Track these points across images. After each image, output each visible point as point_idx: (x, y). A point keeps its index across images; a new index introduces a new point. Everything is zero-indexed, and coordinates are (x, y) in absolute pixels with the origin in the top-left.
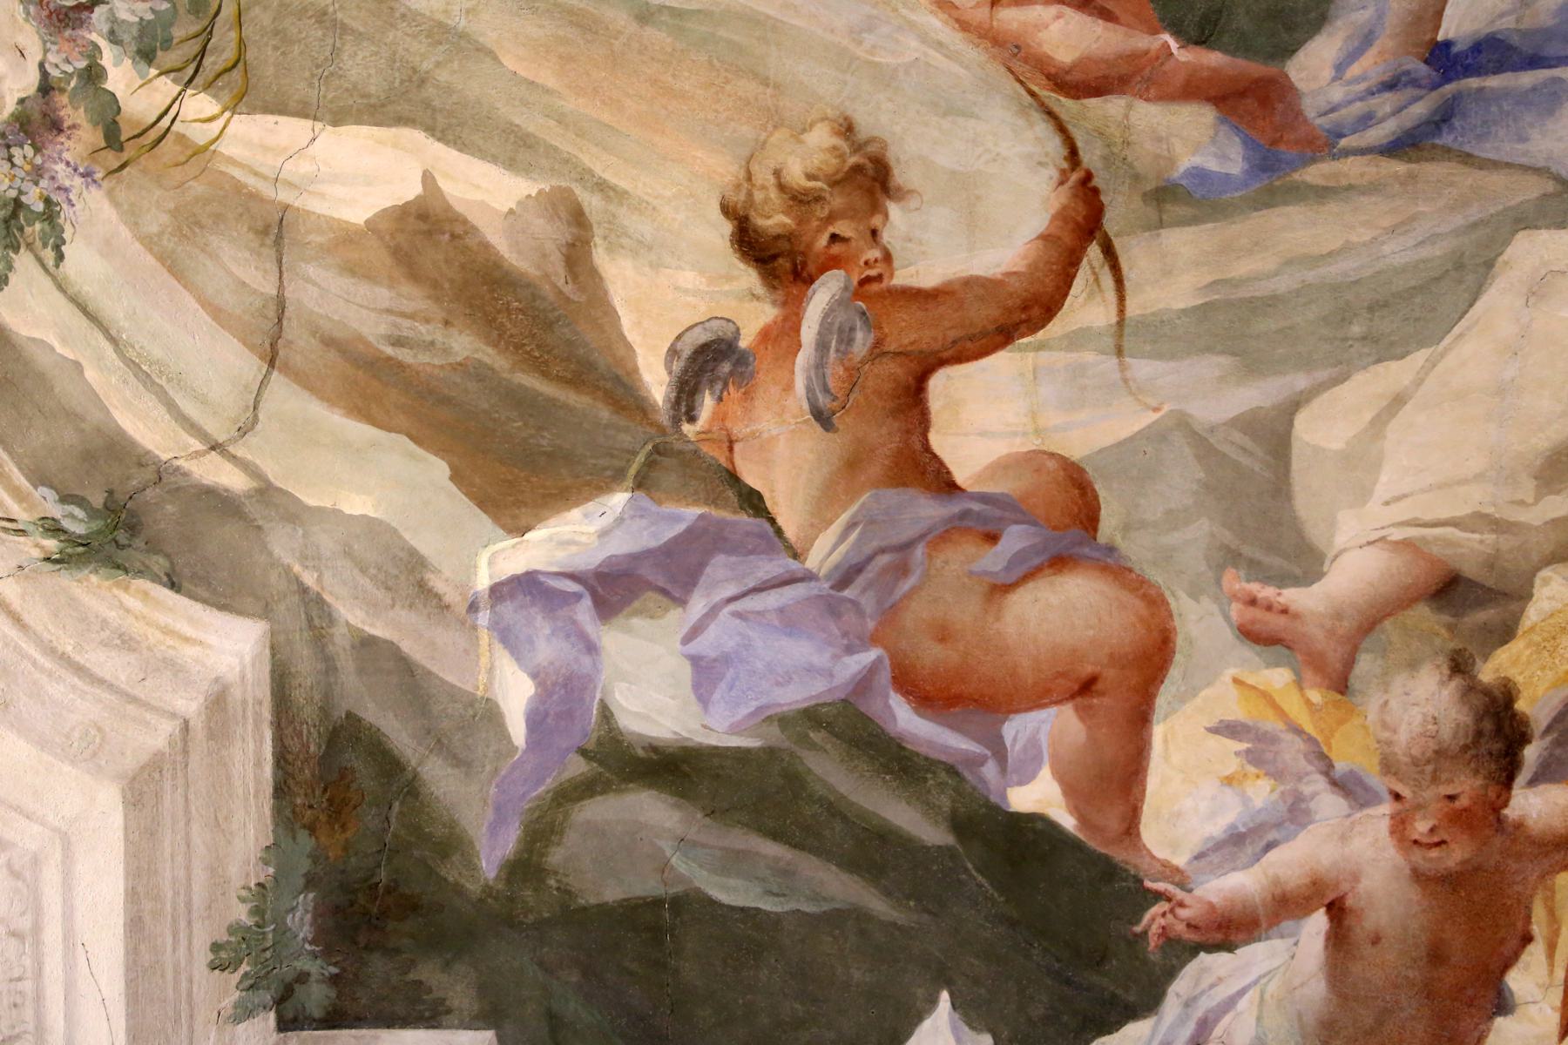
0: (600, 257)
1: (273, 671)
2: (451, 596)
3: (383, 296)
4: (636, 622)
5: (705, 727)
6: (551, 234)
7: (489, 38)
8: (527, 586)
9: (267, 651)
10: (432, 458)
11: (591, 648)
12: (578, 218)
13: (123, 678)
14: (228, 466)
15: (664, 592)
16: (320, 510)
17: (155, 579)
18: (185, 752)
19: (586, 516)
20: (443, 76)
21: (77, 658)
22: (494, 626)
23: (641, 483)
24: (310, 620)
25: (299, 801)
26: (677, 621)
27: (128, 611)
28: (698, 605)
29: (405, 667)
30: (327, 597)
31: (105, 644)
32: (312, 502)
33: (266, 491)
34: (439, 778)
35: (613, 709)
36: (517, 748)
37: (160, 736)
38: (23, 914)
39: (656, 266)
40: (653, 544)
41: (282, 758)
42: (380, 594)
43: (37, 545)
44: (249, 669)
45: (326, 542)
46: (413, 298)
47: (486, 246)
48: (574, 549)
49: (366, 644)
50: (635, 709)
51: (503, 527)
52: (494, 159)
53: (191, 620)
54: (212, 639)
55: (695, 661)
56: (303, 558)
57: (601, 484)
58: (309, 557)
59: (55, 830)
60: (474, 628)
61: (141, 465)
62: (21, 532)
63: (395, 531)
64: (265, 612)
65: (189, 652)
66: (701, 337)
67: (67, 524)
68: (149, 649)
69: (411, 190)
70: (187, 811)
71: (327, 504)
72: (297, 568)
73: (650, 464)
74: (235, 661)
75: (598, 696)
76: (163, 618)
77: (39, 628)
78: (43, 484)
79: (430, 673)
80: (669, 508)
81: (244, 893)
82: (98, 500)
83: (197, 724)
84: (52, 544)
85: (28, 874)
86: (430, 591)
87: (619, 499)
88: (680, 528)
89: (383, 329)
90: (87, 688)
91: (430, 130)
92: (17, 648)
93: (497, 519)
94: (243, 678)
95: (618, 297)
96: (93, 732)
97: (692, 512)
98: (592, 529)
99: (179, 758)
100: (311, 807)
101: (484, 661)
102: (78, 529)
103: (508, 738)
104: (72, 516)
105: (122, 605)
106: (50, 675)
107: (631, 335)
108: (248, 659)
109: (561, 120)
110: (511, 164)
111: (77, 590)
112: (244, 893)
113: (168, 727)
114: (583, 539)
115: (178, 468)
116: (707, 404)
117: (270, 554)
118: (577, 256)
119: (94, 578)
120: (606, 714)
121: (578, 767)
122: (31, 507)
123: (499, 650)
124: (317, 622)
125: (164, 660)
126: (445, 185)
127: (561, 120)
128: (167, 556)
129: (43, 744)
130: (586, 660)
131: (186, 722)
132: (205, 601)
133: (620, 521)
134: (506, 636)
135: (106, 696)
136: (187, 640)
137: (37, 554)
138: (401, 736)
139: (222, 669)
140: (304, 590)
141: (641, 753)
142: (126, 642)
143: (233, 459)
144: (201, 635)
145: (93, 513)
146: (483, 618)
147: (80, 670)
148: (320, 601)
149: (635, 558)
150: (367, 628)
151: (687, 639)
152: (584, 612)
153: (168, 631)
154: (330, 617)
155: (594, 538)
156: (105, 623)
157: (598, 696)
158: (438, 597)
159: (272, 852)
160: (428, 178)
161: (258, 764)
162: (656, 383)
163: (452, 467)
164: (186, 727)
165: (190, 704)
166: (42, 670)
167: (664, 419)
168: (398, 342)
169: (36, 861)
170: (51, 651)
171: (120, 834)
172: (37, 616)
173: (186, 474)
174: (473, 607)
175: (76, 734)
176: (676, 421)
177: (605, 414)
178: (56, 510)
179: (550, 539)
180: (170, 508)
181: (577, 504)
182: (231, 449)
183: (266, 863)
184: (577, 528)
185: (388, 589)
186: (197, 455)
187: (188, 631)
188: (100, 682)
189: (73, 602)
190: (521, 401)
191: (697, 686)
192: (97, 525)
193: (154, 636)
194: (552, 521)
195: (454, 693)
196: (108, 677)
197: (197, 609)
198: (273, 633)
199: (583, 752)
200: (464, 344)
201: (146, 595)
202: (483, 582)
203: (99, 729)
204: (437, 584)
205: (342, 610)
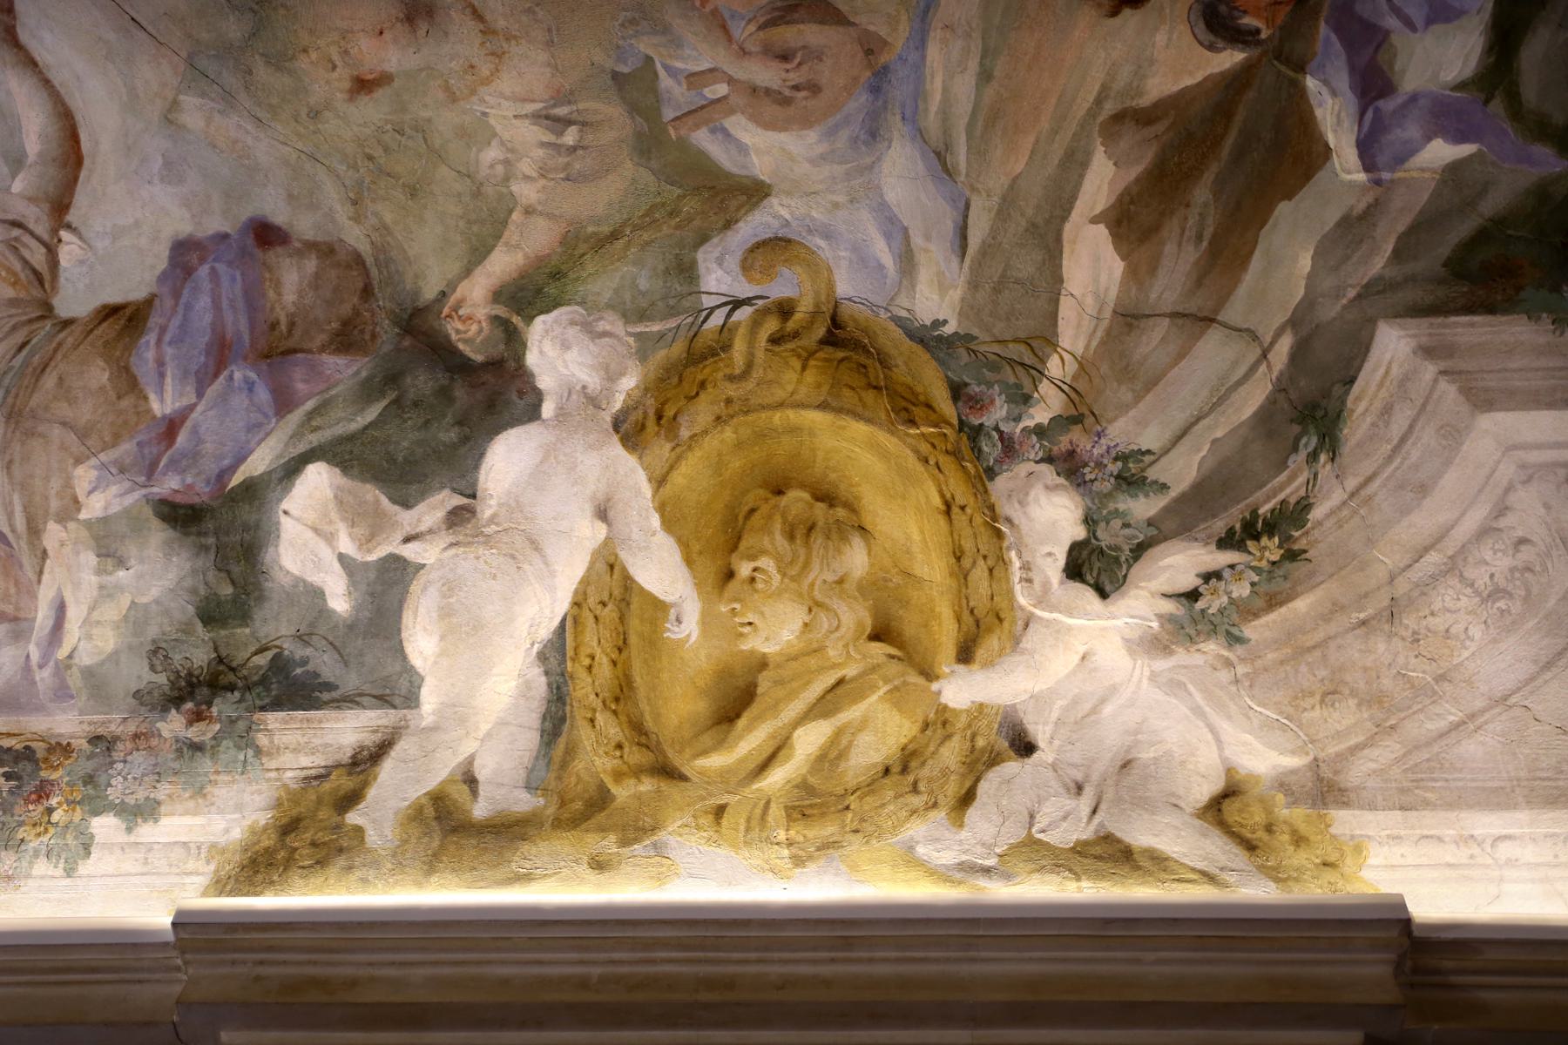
0: (1145, 101)
1: (1412, 317)
2: (1369, 198)
3: (1170, 248)
4: (1397, 67)
5: (1478, 12)
6: (1130, 137)
7: (1005, 181)
8: (1367, 148)
9: (1398, 320)
10: (1276, 213)
11: (1414, 98)
12: (1119, 118)
13: (1409, 413)
14: (1277, 347)
15: (1379, 46)
16: (1307, 287)
17: (1347, 392)
18: (1460, 373)
19: (1320, 105)
20: (1030, 212)
21: (1395, 442)
22: (1393, 170)
23: (1301, 68)
24: (1379, 293)
25: (1499, 298)
26: (1400, 38)
27: (1367, 410)
28: (1391, 22)
29: (1413, 229)
30: (1365, 281)
31: (1387, 424)
32: (1302, 292)
33: (1294, 322)
34: (1494, 203)
35: (1459, 80)
36: (1480, 150)
37: (1449, 391)
38: (1556, 474)
39: (1152, 62)
40: (1344, 57)
41: (1469, 310)
42: (1364, 247)
43: (1324, 466)
44: (1412, 332)
45: (1328, 283)
46: (1171, 227)
47: (1137, 180)
48: (1343, 114)
49: (1398, 255)
50: (1460, 65)
51: (1325, 163)
52: (1082, 176)
53: (1374, 370)
54: (1388, 356)
55: (1430, 22)
56: (1338, 297)
57: (1300, 93)
58: (1338, 293)
59: (1503, 455)
60: (1392, 181)
61: (1275, 402)
62: (1316, 475)
63: (1325, 236)
64: (1371, 323)
65: (1395, 371)
66: (1201, 27)
67: (1310, 449)
68: (1391, 396)
69: (1102, 231)
70: (1499, 371)
71: (1303, 283)
72: (1344, 301)
73: (1287, 62)
74: (1403, 341)
75: (1448, 92)
76: (1373, 388)
77: (1376, 465)
78: (1286, 462)
79: (1420, 212)
80: (1319, 47)
81: (1558, 333)
82: (1296, 429)
83: (1443, 365)
84: (1323, 457)
85: (1531, 471)
86: (1364, 212)
87: (1311, 83)
88: (1334, 37)
89: (1191, 248)
90: (1414, 436)
91: (1064, 219)
92: (1388, 479)
93: (1320, 167)
94: (1415, 336)
95: (1172, 87)
96: (1443, 432)
97: (1322, 24)
98: (1330, 101)
99: (1464, 377)
100: (1504, 290)
101: (1415, 174)
102: (1314, 440)
103: (1471, 156)
104: (1306, 445)
105: (1363, 414)
106: (1404, 459)
107: (1199, 77)
108: (1402, 333)
109: (1055, 132)
110: (1085, 165)
111: (1352, 442)
112: (1558, 333)
113: (1443, 385)
114: (1337, 108)
115: (1278, 379)
116: (1248, 21)
117: (1335, 319)
118: (1144, 117)
119: (1345, 431)
120: (1461, 86)
121: (1497, 106)
122: (1300, 470)
123: (1407, 165)
124: (1381, 288)
125: (1399, 387)
126: (1099, 208)
127: (1055, 132)
128: (1333, 385)
129: (1448, 463)
130: (1422, 102)
131: (1441, 372)
132: (1363, 361)
133: (1326, 82)
134: (1400, 160)
135: (1420, 424)
136: (1387, 372)
137: (1328, 467)
138: (1462, 230)
139: (1408, 350)
140: (1359, 296)
141: (1492, 60)
142: (1387, 410)
143: (1272, 344)
144: (1385, 363)
145: (1304, 432)
146: (1386, 176)
147: (1403, 440)
148: (1367, 286)
149: (1352, 69)
150: (1387, 255)
151: (1410, 25)
152: (1388, 105)
153: (1381, 385)
154: (1378, 279)
155: (1337, 100)
156: (1374, 424)
157: (1448, 92)
158: (1369, 207)
159: (1533, 315)
160: (1095, 220)
161: (1472, 325)
162: (1230, 58)
163: (1282, 199)
164: (1443, 373)
165: (1429, 370)
166: (1402, 463)
167: (1257, 51)
168: (1199, 238)
169: (1523, 466)
170: (1390, 459)
171: (1510, 414)
172: (1367, 468)
173: (1281, 373)
174: (1378, 182)
175: (1444, 442)
176: (1259, 43)
177: (1251, 94)
178: (1302, 455)
179: (1335, 131)
180: (1302, 384)
181: (1312, 112)
182: (1266, 345)
183: (1539, 318)
184: (1329, 111)
185: (1362, 241)
186: (1269, 366)
187: (1382, 371)
188: (1411, 427)
189: (1359, 445)
190: (1239, 154)
191: (1448, 20)
192: (1312, 429)
193: (1383, 394)
194: (1323, 129)
195: (1436, 194)
196: (1408, 422)
197: (1368, 367)
198: (1386, 317)
199: (1486, 102)
200: (1201, 193)
201: (1358, 399)
202: (1361, 177)
203: (1442, 427)
204: (1361, 206)
205: (1374, 271)
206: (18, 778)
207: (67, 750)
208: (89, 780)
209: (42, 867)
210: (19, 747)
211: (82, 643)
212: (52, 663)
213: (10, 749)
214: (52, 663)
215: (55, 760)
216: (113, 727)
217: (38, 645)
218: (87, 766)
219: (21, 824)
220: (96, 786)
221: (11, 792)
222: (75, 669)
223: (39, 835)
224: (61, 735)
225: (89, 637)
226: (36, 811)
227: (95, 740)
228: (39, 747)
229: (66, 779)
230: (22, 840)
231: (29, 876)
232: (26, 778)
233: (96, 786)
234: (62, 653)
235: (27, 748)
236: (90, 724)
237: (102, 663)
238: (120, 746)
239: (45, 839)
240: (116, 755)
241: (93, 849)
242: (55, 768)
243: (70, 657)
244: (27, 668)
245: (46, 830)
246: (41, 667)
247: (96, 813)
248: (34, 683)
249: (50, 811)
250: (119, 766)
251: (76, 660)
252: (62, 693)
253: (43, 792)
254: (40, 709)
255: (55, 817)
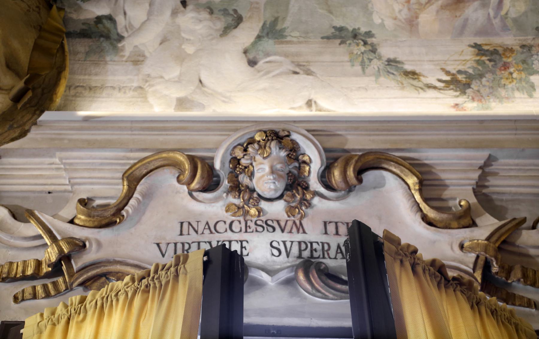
206: (495, 61)
207: (512, 50)
208: (524, 62)
209: (517, 94)
210: (491, 49)
211: (511, 8)
212: (499, 17)
213: (488, 50)
214: (499, 17)
215: (508, 54)
216: (529, 42)
217: (493, 9)
218: (523, 57)
219: (501, 78)
220: (528, 64)
221: (492, 66)
222: (509, 19)
223: (510, 83)
224: (508, 45)
225: (514, 6)
226: (506, 74)
227: (523, 46)
228: (500, 50)
229: (514, 62)
230: (505, 85)
231: (514, 97)
232: (498, 61)
233: (528, 64)
234: (503, 13)
235: (495, 50)
236: (519, 40)
237: (520, 16)
238: (534, 48)
239: (514, 84)
240: (533, 52)
241: (536, 88)
242: (509, 57)
243: (507, 14)
244: (489, 18)
245: (513, 81)
246: (495, 18)
247: (531, 74)
248: (492, 24)
249: (511, 74)
250: (535, 57)
251: (509, 15)
252: (505, 28)
253: (506, 66)
254: (497, 34)
255: (515, 75)
